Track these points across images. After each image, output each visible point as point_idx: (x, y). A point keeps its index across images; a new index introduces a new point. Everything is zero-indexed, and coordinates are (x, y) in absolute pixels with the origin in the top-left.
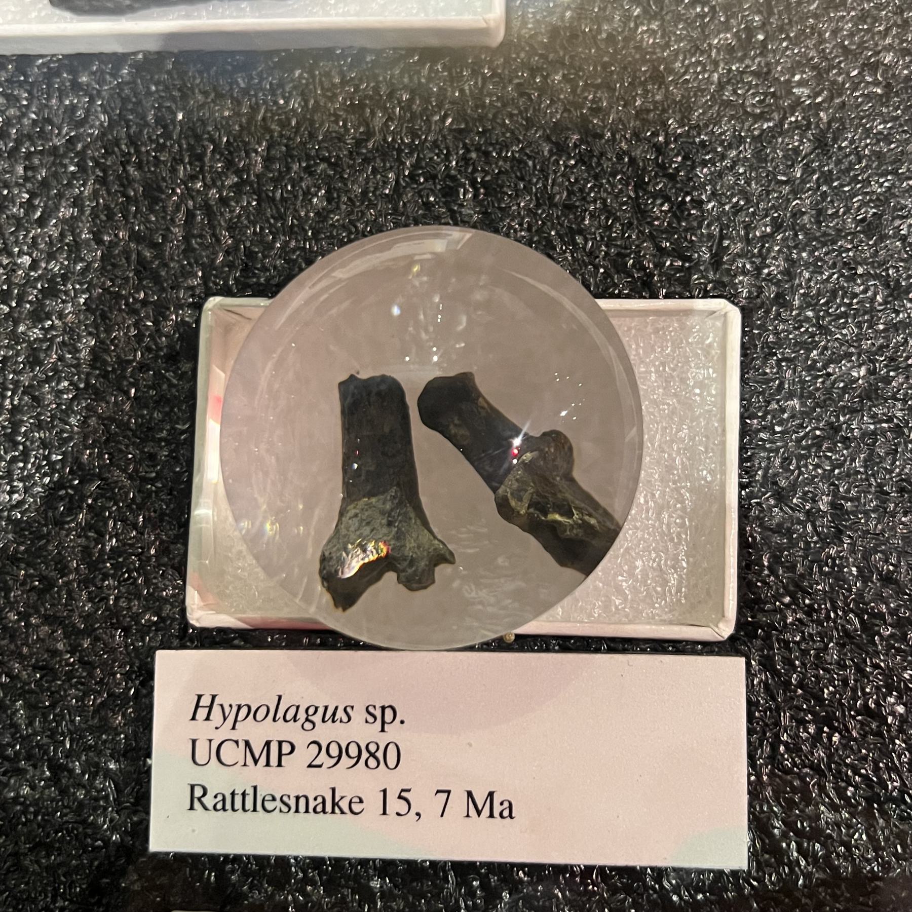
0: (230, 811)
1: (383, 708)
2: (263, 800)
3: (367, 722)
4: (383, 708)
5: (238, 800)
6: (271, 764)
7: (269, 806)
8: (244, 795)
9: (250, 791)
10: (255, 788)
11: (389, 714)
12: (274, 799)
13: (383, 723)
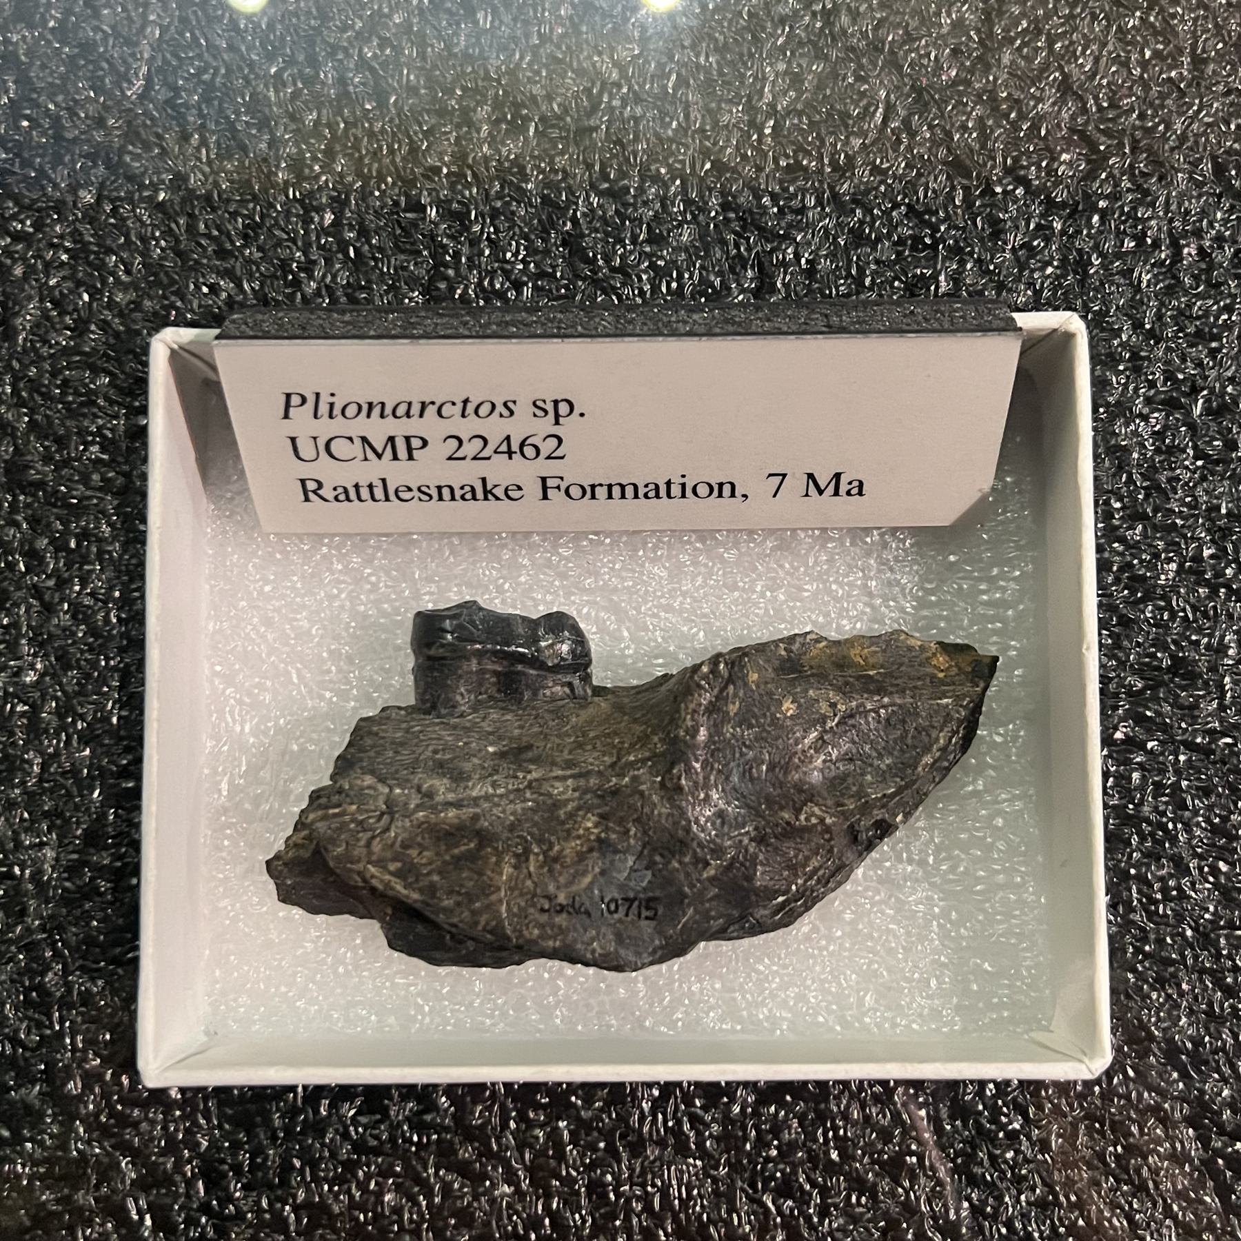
0: (356, 502)
1: (556, 402)
2: (397, 491)
3: (535, 415)
4: (556, 402)
6: (400, 456)
8: (371, 486)
9: (380, 484)
10: (384, 480)
11: (564, 408)
12: (410, 489)
13: (557, 416)
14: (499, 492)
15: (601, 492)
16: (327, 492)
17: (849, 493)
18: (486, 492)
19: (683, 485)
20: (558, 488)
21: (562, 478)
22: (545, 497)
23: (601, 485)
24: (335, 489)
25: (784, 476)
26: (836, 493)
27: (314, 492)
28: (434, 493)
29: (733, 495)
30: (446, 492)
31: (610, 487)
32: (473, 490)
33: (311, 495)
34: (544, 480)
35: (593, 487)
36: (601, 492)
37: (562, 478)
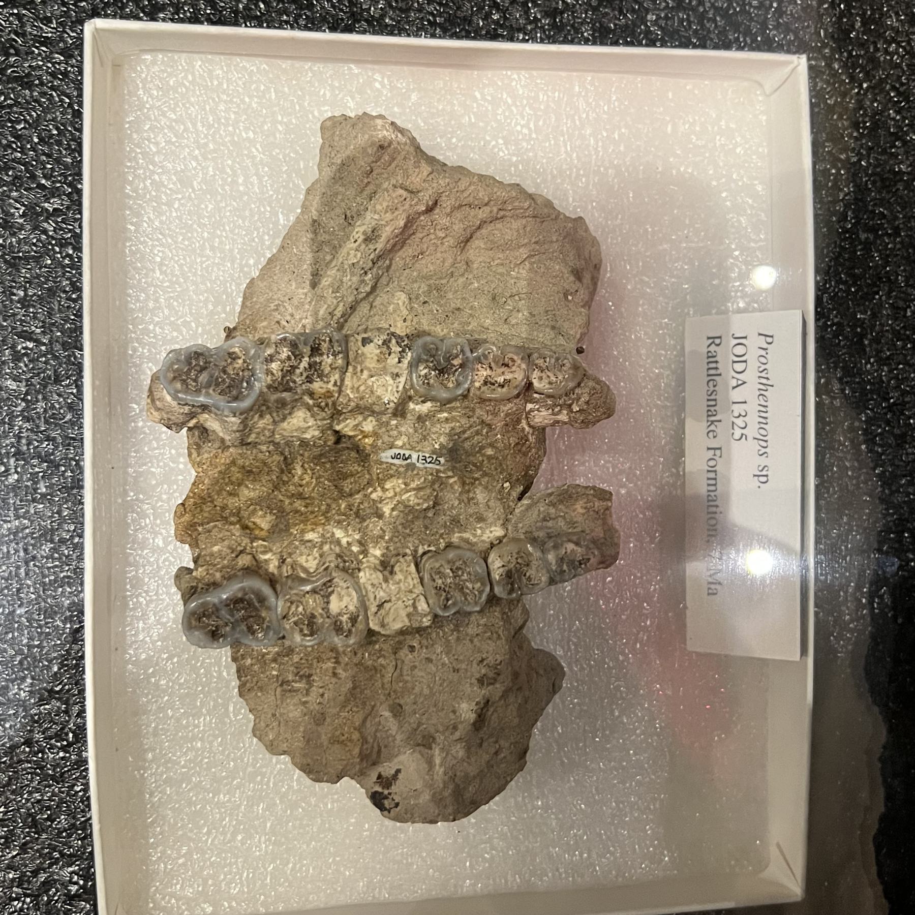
0: (707, 361)
5: (713, 365)
7: (711, 383)
8: (716, 368)
9: (718, 372)
10: (720, 375)
14: (712, 427)
15: (712, 475)
16: (713, 348)
17: (709, 589)
18: (712, 422)
22: (709, 449)
27: (713, 342)
28: (713, 397)
30: (713, 403)
31: (715, 479)
33: (711, 341)
34: (720, 449)
36: (712, 475)
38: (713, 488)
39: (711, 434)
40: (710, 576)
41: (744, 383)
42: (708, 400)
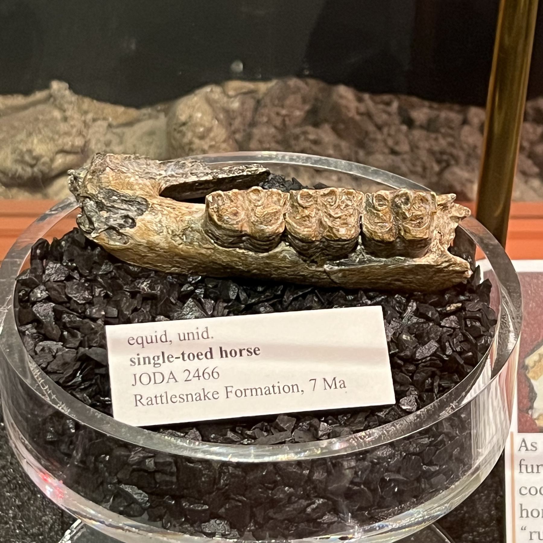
7: (173, 400)
10: (166, 393)
14: (210, 396)
18: (205, 396)
19: (279, 387)
20: (231, 392)
21: (232, 387)
22: (227, 397)
23: (248, 389)
24: (147, 399)
25: (315, 380)
26: (336, 388)
27: (139, 401)
28: (185, 397)
29: (298, 391)
30: (190, 397)
32: (200, 396)
33: (138, 402)
34: (226, 388)
35: (245, 390)
37: (232, 387)
38: (259, 391)
39: (216, 396)
40: (330, 387)
41: (171, 373)
42: (187, 401)
